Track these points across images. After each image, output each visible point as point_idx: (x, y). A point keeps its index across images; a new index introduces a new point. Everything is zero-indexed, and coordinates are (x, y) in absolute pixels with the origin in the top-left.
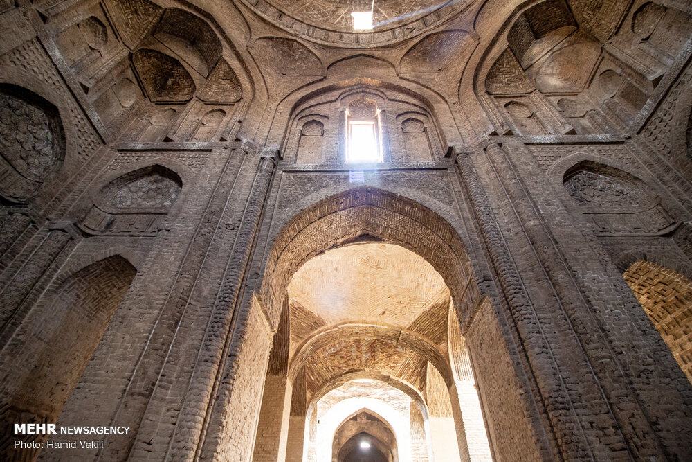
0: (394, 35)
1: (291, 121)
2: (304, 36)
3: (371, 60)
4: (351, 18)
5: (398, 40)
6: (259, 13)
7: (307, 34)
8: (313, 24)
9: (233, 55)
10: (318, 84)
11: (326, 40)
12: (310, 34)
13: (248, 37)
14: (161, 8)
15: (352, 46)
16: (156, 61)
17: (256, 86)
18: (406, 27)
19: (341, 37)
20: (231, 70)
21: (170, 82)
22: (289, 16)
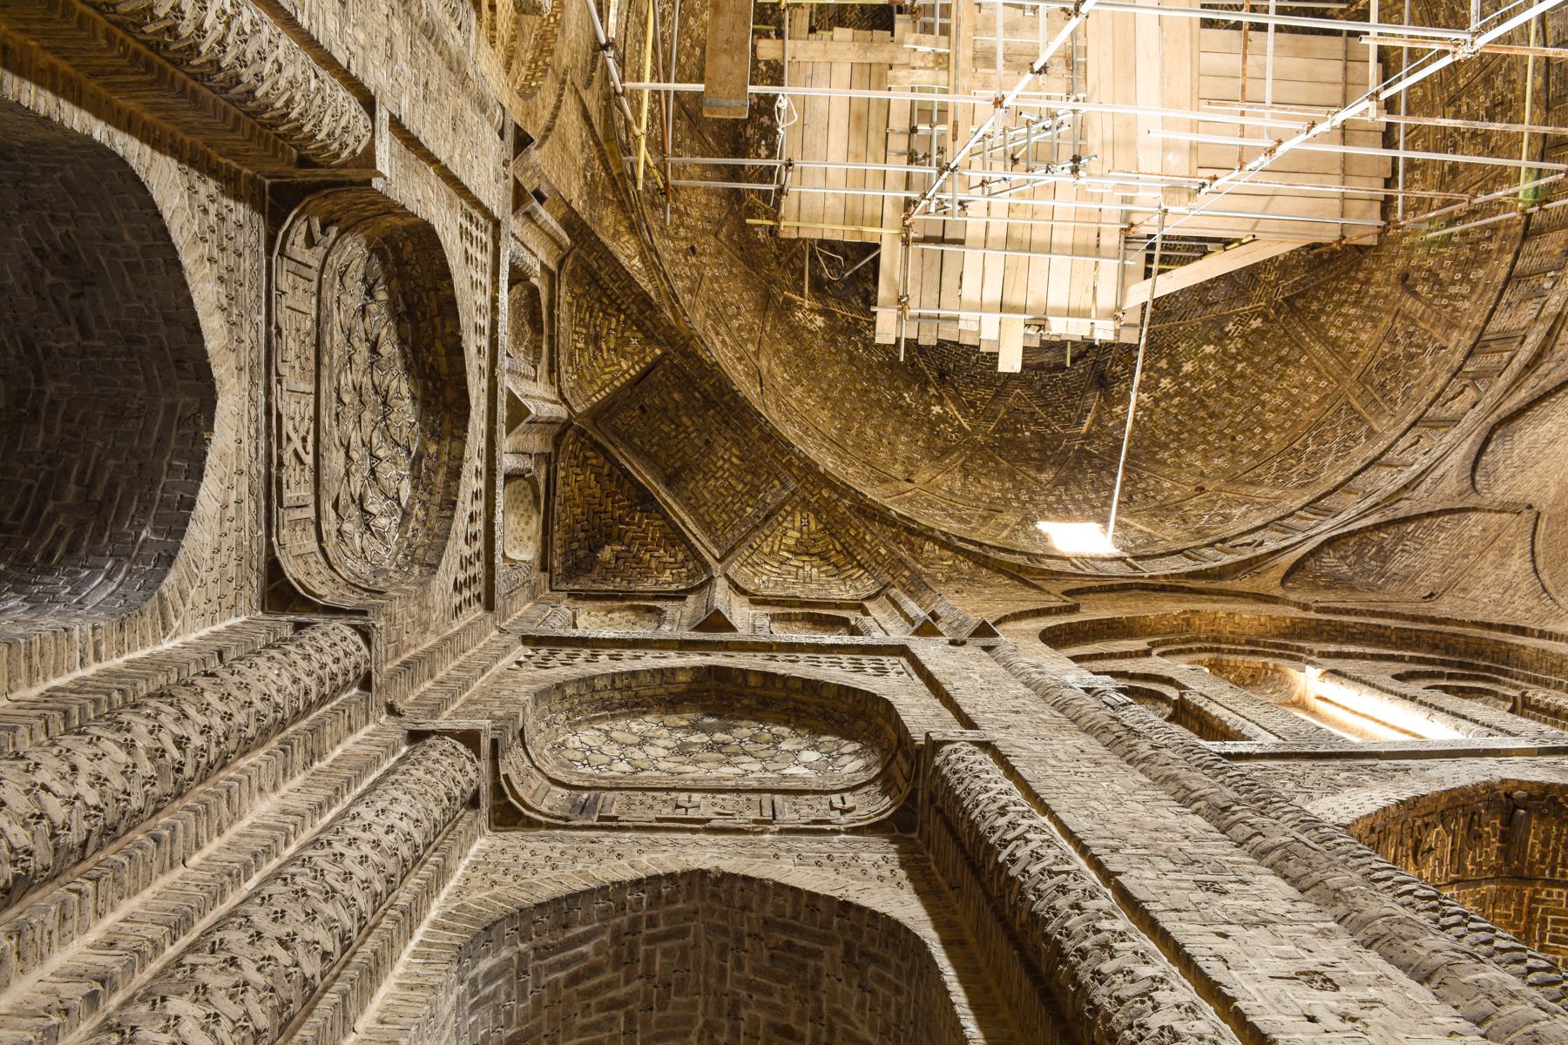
16: (593, 483)
21: (606, 553)
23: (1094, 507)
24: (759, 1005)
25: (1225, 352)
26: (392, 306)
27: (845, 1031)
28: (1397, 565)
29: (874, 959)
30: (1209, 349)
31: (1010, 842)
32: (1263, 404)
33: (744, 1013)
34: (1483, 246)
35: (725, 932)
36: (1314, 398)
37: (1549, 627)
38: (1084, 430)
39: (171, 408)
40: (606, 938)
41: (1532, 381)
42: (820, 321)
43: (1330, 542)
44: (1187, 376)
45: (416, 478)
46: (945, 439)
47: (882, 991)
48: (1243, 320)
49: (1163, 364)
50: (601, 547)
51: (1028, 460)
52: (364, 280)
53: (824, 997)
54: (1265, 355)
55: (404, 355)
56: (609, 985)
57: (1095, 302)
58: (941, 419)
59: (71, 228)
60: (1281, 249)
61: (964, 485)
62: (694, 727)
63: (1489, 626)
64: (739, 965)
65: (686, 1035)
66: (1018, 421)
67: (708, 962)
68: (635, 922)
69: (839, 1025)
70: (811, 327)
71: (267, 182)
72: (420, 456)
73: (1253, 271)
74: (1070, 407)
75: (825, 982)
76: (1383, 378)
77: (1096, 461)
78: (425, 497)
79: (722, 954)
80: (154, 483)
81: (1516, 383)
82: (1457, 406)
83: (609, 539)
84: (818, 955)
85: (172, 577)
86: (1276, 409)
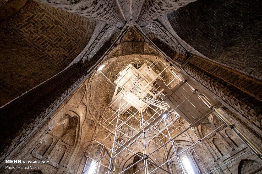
21: (131, 33)
24: (66, 39)
26: (169, 47)
27: (56, 49)
28: (80, 94)
29: (63, 60)
31: (67, 92)
33: (66, 36)
34: (102, 113)
35: (78, 41)
37: (65, 106)
39: (183, 30)
40: (86, 29)
41: (88, 111)
42: (136, 59)
43: (86, 89)
45: (152, 33)
47: (59, 59)
48: (109, 91)
50: (132, 33)
51: (111, 67)
52: (174, 48)
53: (62, 49)
54: (106, 91)
55: (164, 43)
56: (80, 24)
57: (120, 82)
58: (120, 63)
59: (210, 41)
60: (113, 98)
62: (106, 40)
63: (69, 101)
64: (73, 40)
65: (67, 26)
67: (76, 36)
68: (86, 33)
69: (58, 49)
71: (191, 55)
72: (154, 35)
73: (113, 94)
75: (64, 51)
76: (97, 100)
78: (150, 33)
79: (76, 39)
80: (178, 22)
81: (89, 109)
82: (90, 104)
83: (132, 34)
84: (68, 52)
85: (167, 18)
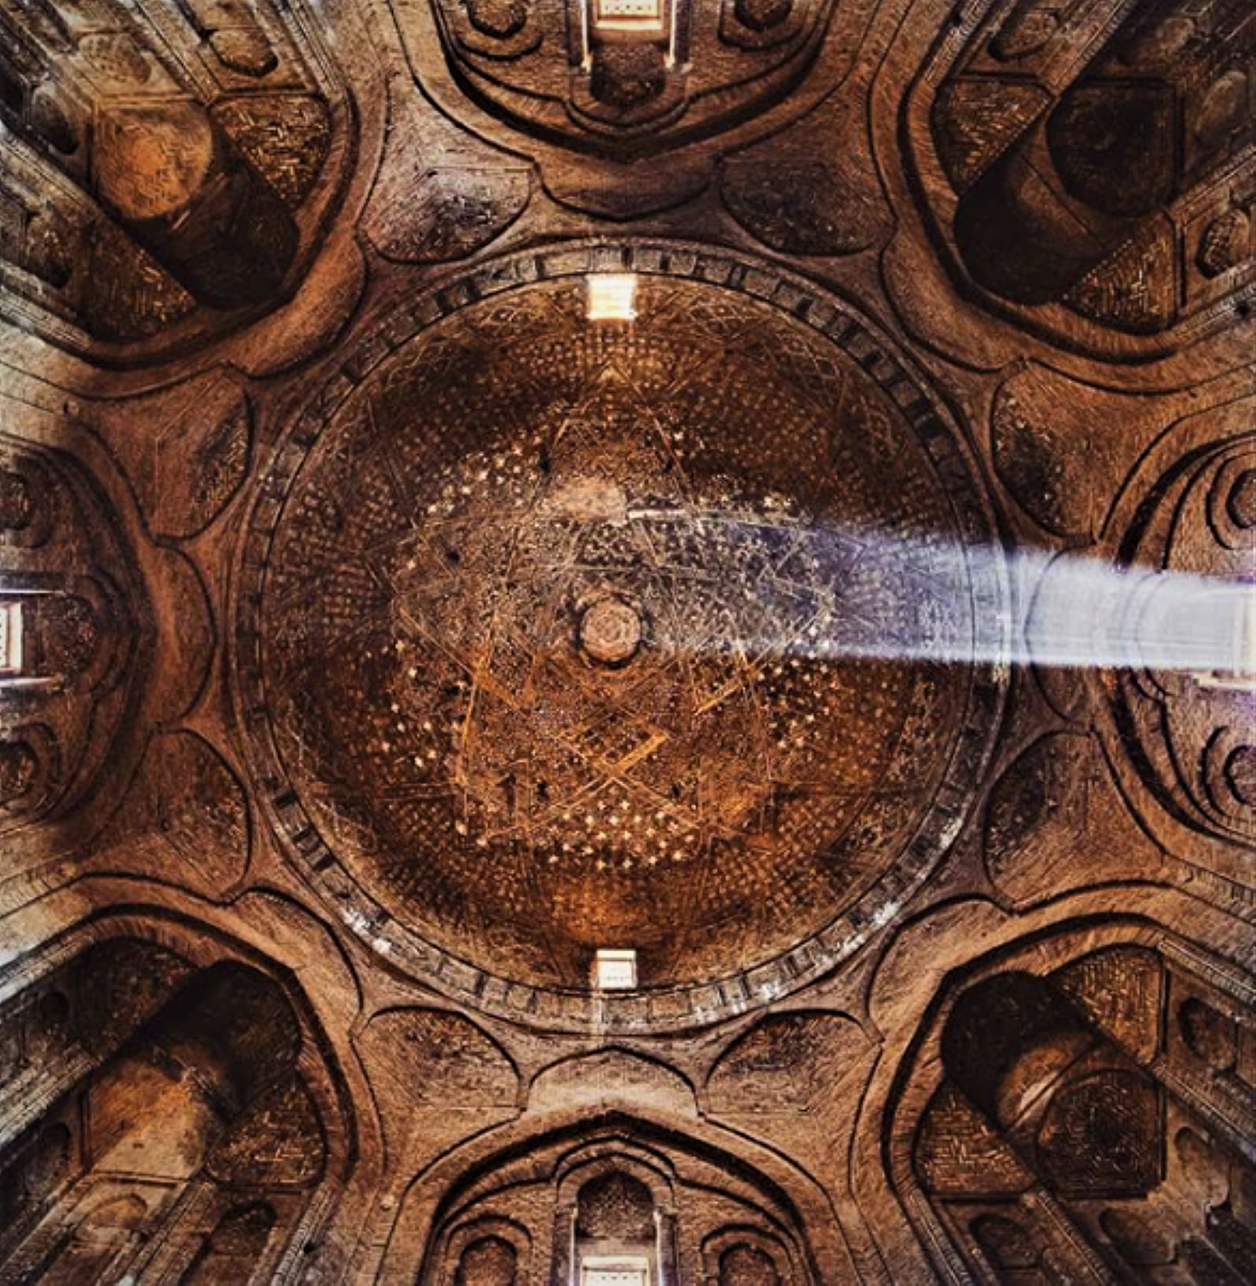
0: (540, 267)
1: (821, 26)
2: (754, 263)
3: (597, 208)
4: (637, 306)
5: (532, 252)
6: (851, 311)
7: (746, 268)
8: (728, 293)
9: (932, 204)
10: (737, 141)
11: (701, 257)
12: (739, 269)
13: (887, 253)
14: (1064, 304)
15: (642, 241)
17: (892, 124)
18: (512, 283)
19: (665, 264)
20: (945, 166)
22: (785, 310)
23: (582, 340)
25: (456, 487)
30: (466, 490)
32: (439, 433)
36: (407, 430)
38: (567, 422)
44: (485, 467)
46: (677, 407)
49: (500, 480)
58: (676, 428)
61: (678, 359)
66: (614, 430)
70: (776, 495)
74: (572, 444)
77: (565, 390)
86: (432, 425)
